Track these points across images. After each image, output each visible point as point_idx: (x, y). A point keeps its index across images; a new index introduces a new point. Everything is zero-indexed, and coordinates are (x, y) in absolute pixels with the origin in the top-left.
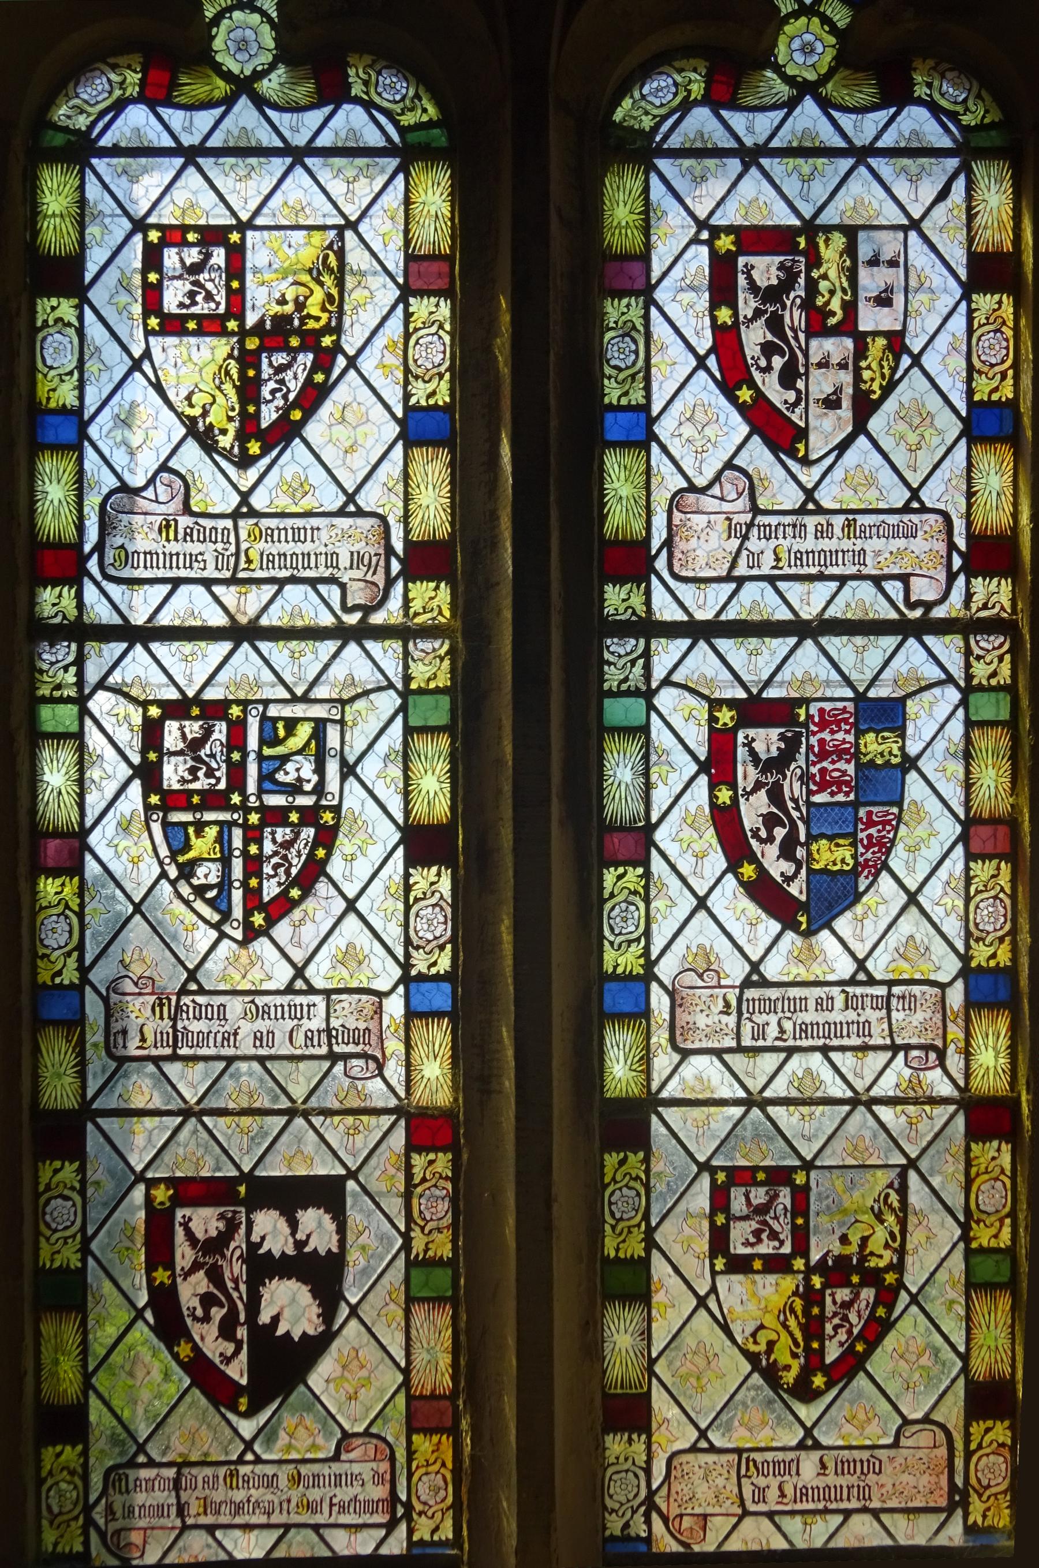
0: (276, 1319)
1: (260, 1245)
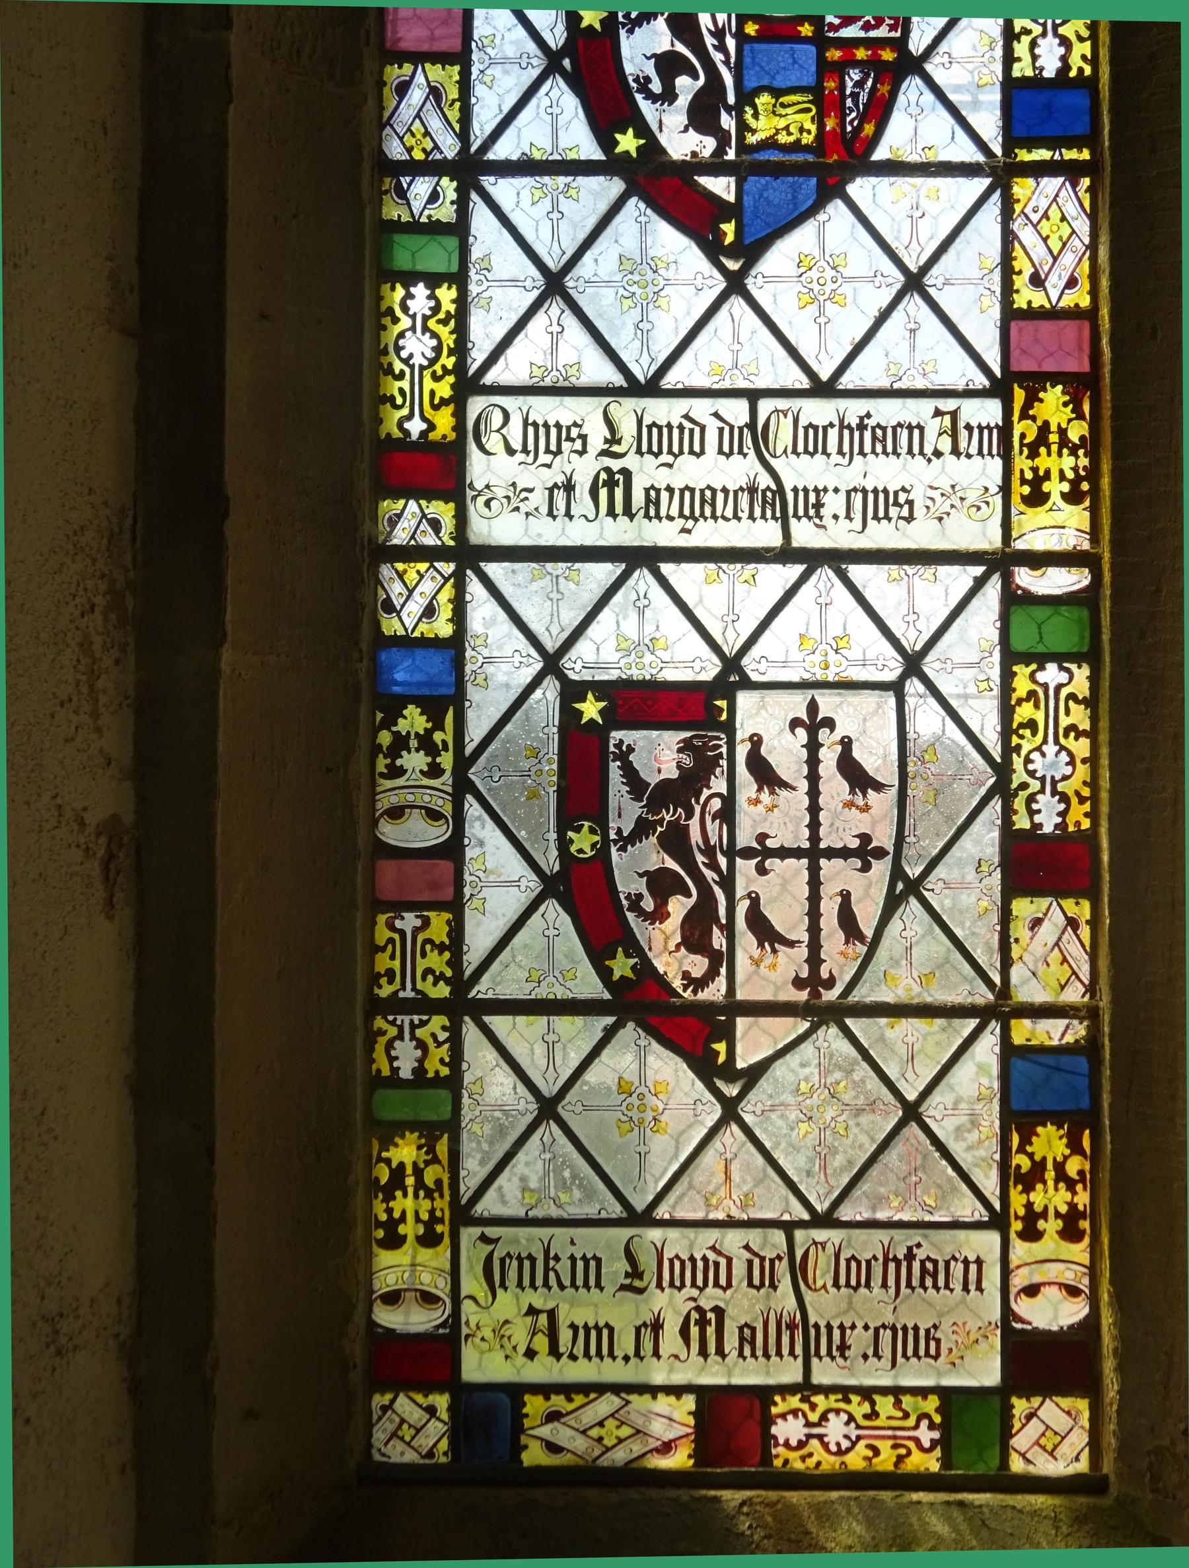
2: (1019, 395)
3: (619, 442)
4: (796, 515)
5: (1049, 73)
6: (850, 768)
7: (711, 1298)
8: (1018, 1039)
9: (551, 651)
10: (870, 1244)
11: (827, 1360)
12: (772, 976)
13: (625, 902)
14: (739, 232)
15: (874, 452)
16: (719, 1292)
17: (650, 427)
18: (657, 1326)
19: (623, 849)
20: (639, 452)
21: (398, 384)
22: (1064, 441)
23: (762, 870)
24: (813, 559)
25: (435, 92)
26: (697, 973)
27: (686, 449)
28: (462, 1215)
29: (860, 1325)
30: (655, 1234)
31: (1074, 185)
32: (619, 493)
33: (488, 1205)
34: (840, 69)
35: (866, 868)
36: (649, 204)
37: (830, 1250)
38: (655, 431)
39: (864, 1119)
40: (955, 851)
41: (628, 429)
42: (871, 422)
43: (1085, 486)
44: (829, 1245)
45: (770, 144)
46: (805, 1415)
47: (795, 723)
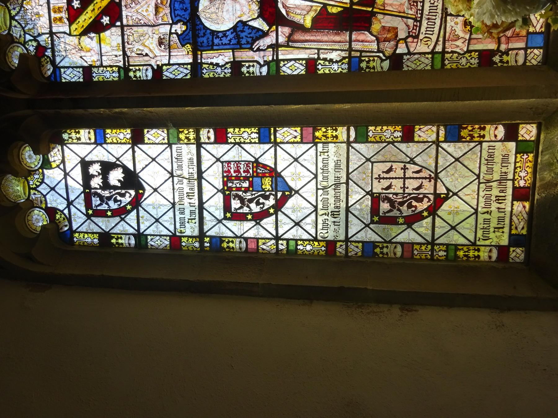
0: (119, 181)
1: (100, 186)
2: (317, 140)
3: (326, 213)
4: (339, 181)
5: (257, 136)
6: (389, 171)
7: (493, 198)
8: (443, 139)
9: (365, 226)
10: (484, 168)
11: (508, 176)
12: (428, 186)
13: (413, 213)
14: (287, 191)
15: (327, 167)
16: (492, 196)
17: (323, 208)
18: (499, 208)
19: (403, 213)
20: (328, 209)
21: (315, 251)
22: (326, 132)
23: (407, 188)
24: (348, 178)
25: (264, 244)
26: (427, 200)
27: (327, 201)
28: (474, 244)
29: (501, 170)
30: (480, 209)
31: (278, 131)
32: (335, 213)
33: (472, 238)
34: (258, 173)
35: (407, 168)
36: (282, 207)
37: (484, 175)
38: (324, 207)
39: (458, 169)
40: (405, 152)
41: (323, 212)
42: (322, 168)
43: (334, 128)
44: (484, 175)
45: (271, 186)
46: (519, 180)
47: (379, 182)
